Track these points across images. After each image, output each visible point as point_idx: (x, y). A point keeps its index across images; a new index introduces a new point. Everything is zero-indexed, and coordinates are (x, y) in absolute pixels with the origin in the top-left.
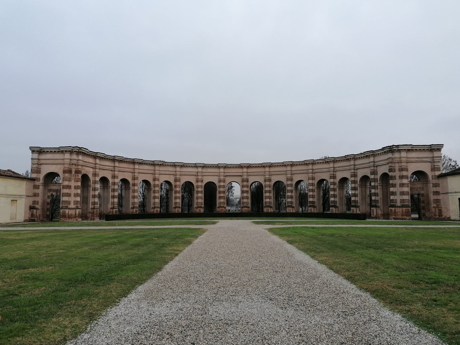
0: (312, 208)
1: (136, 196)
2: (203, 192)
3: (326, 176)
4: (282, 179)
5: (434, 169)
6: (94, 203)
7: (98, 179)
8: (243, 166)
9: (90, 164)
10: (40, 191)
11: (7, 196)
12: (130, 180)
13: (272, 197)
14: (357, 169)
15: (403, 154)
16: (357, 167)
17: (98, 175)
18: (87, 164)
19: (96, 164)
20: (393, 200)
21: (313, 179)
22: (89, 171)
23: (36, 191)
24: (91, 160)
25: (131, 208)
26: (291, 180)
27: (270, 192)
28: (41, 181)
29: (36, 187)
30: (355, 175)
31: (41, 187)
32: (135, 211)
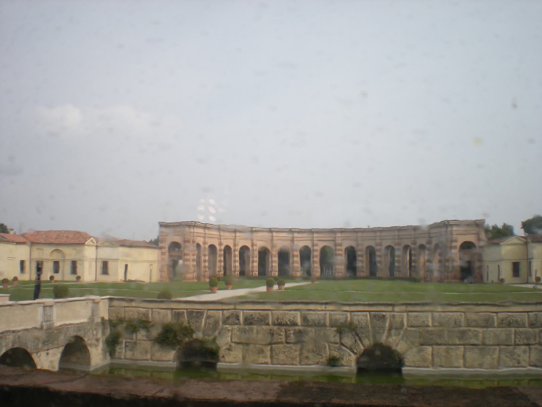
0: (398, 273)
1: (237, 260)
2: (299, 256)
3: (408, 242)
4: (372, 243)
5: (479, 239)
6: (205, 267)
7: (207, 246)
8: (335, 231)
9: (201, 234)
10: (166, 256)
11: (149, 261)
12: (232, 246)
13: (365, 261)
14: (432, 237)
15: (455, 228)
16: (432, 235)
17: (207, 243)
18: (199, 234)
19: (205, 234)
20: (446, 266)
21: (399, 244)
22: (200, 240)
23: (163, 257)
24: (201, 231)
25: (234, 271)
26: (380, 245)
27: (362, 256)
28: (167, 249)
29: (163, 254)
30: (429, 243)
31: (167, 254)
32: (236, 274)
